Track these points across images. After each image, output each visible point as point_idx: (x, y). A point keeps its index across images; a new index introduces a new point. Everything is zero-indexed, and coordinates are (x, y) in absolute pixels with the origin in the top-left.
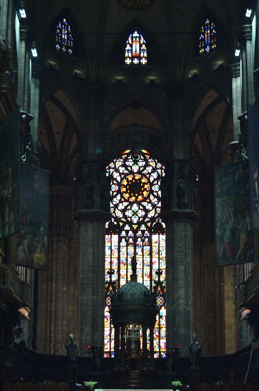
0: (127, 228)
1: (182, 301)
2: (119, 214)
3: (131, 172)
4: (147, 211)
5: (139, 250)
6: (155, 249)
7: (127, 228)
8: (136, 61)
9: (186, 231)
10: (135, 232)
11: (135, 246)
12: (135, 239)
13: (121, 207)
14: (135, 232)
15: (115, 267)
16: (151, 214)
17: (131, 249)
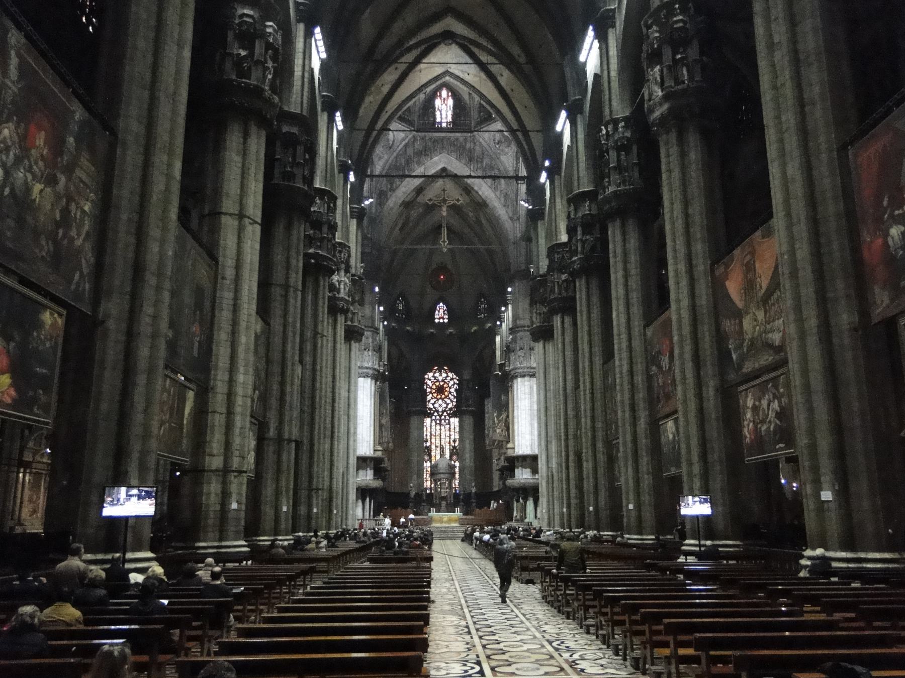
0: (436, 414)
1: (467, 461)
2: (431, 406)
3: (438, 381)
4: (448, 404)
5: (443, 428)
6: (452, 427)
7: (436, 414)
8: (441, 321)
9: (469, 420)
10: (440, 416)
11: (440, 425)
12: (440, 420)
13: (432, 401)
14: (440, 416)
15: (428, 438)
16: (450, 406)
17: (438, 427)
